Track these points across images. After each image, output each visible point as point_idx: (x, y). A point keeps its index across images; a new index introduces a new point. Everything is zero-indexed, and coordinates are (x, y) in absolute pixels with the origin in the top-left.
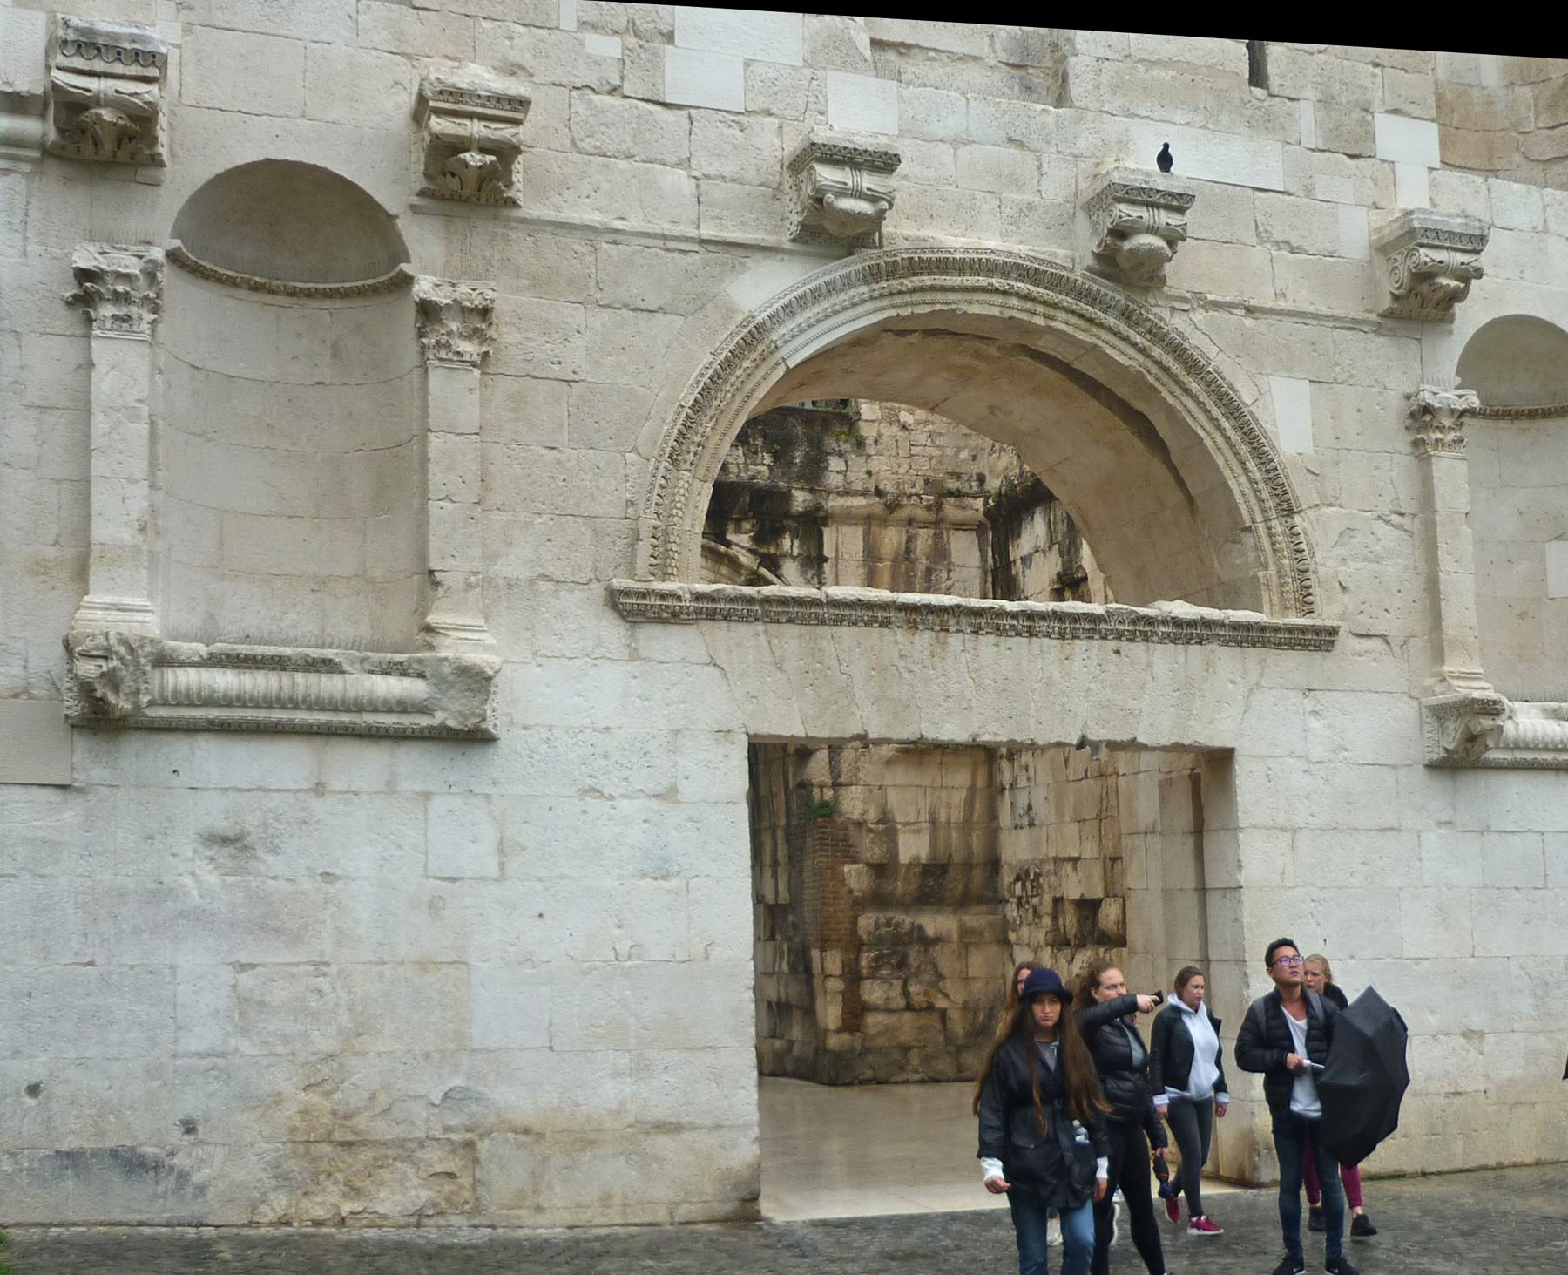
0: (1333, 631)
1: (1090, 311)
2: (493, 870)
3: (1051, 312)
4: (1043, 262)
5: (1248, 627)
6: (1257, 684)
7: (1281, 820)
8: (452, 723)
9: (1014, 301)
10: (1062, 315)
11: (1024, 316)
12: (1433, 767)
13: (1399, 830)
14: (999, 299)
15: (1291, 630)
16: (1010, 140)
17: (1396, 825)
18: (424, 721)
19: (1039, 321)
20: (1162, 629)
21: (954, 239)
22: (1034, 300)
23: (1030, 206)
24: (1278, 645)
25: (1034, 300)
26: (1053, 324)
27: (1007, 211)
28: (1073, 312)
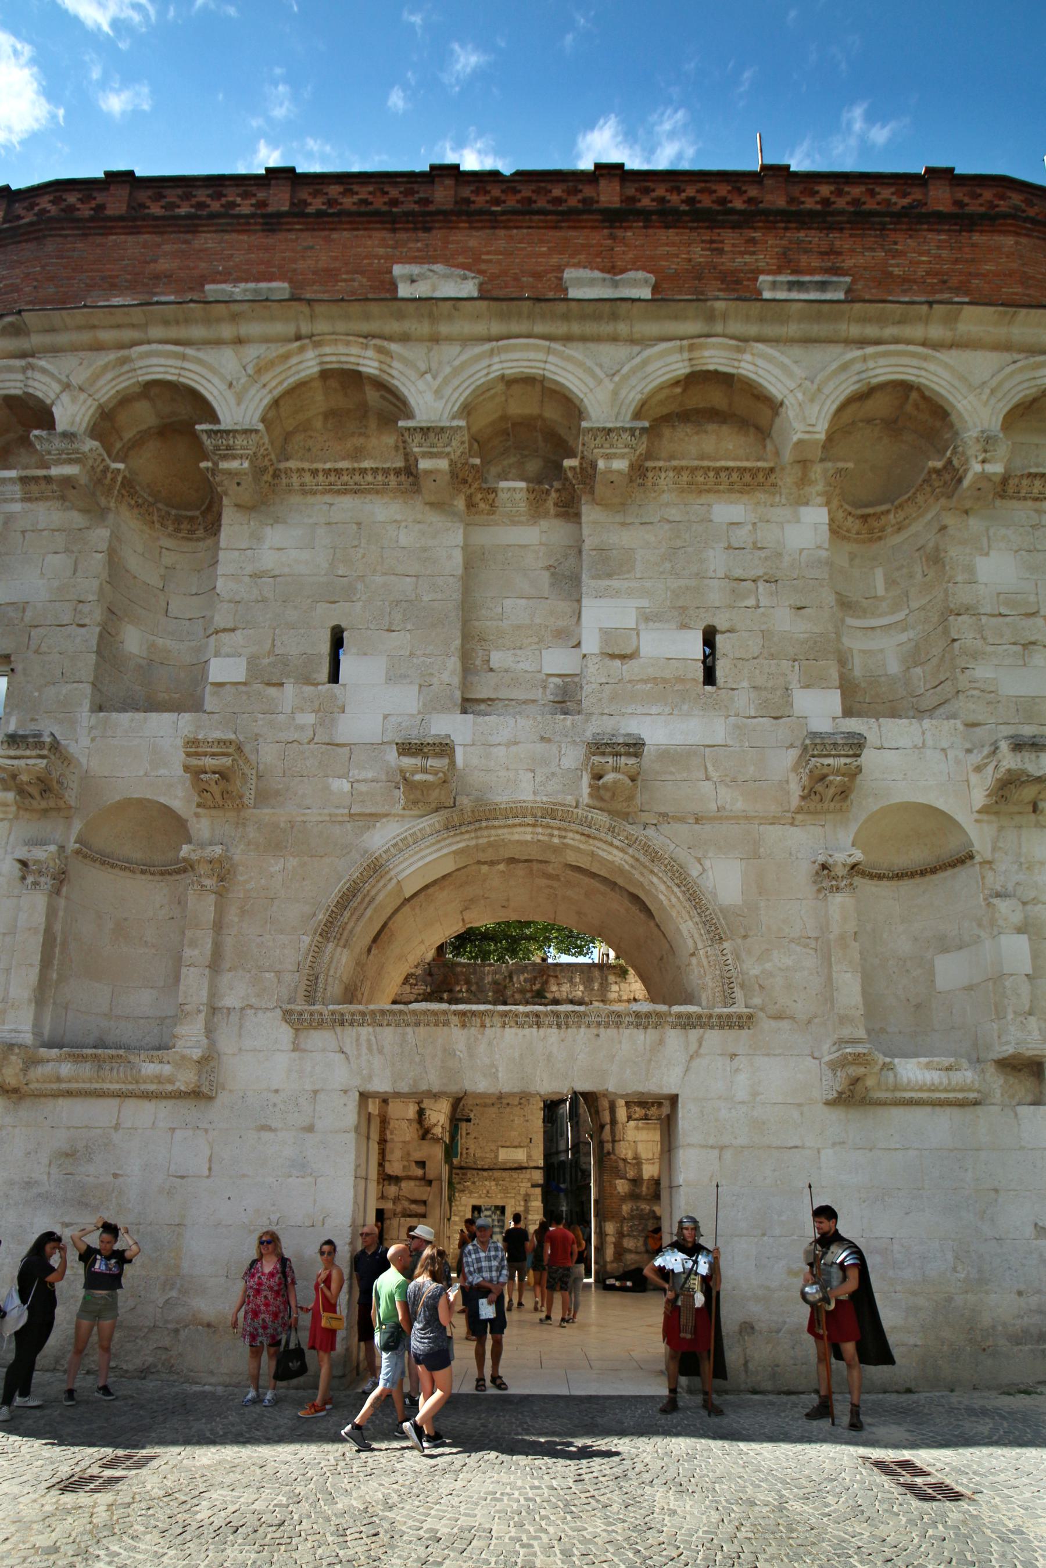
0: (750, 1017)
1: (587, 831)
2: (207, 1173)
3: (563, 833)
4: (555, 804)
5: (689, 1016)
6: (696, 1052)
7: (711, 1141)
8: (183, 1088)
9: (540, 830)
10: (570, 835)
11: (546, 838)
12: (828, 1103)
13: (803, 1147)
14: (530, 829)
15: (720, 1016)
16: (542, 738)
17: (799, 1143)
18: (169, 1088)
19: (556, 840)
20: (627, 1019)
21: (502, 798)
22: (552, 828)
23: (553, 774)
24: (712, 1027)
25: (552, 828)
26: (565, 841)
27: (538, 779)
28: (577, 832)
